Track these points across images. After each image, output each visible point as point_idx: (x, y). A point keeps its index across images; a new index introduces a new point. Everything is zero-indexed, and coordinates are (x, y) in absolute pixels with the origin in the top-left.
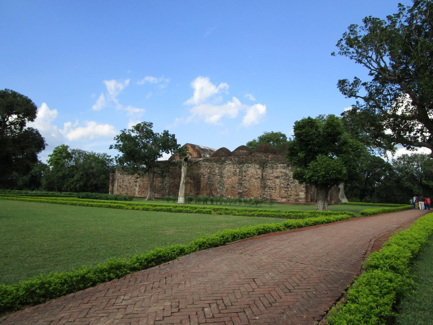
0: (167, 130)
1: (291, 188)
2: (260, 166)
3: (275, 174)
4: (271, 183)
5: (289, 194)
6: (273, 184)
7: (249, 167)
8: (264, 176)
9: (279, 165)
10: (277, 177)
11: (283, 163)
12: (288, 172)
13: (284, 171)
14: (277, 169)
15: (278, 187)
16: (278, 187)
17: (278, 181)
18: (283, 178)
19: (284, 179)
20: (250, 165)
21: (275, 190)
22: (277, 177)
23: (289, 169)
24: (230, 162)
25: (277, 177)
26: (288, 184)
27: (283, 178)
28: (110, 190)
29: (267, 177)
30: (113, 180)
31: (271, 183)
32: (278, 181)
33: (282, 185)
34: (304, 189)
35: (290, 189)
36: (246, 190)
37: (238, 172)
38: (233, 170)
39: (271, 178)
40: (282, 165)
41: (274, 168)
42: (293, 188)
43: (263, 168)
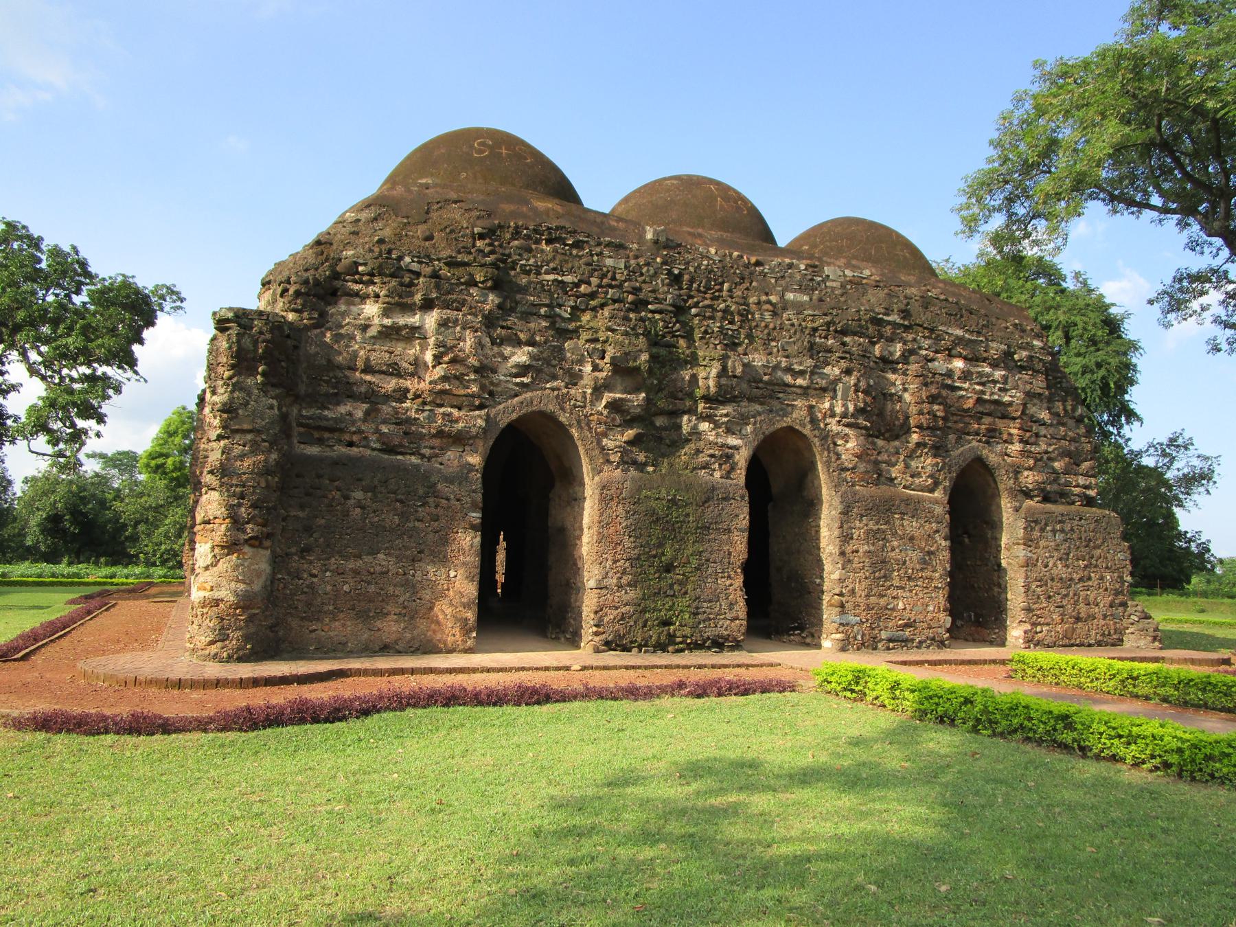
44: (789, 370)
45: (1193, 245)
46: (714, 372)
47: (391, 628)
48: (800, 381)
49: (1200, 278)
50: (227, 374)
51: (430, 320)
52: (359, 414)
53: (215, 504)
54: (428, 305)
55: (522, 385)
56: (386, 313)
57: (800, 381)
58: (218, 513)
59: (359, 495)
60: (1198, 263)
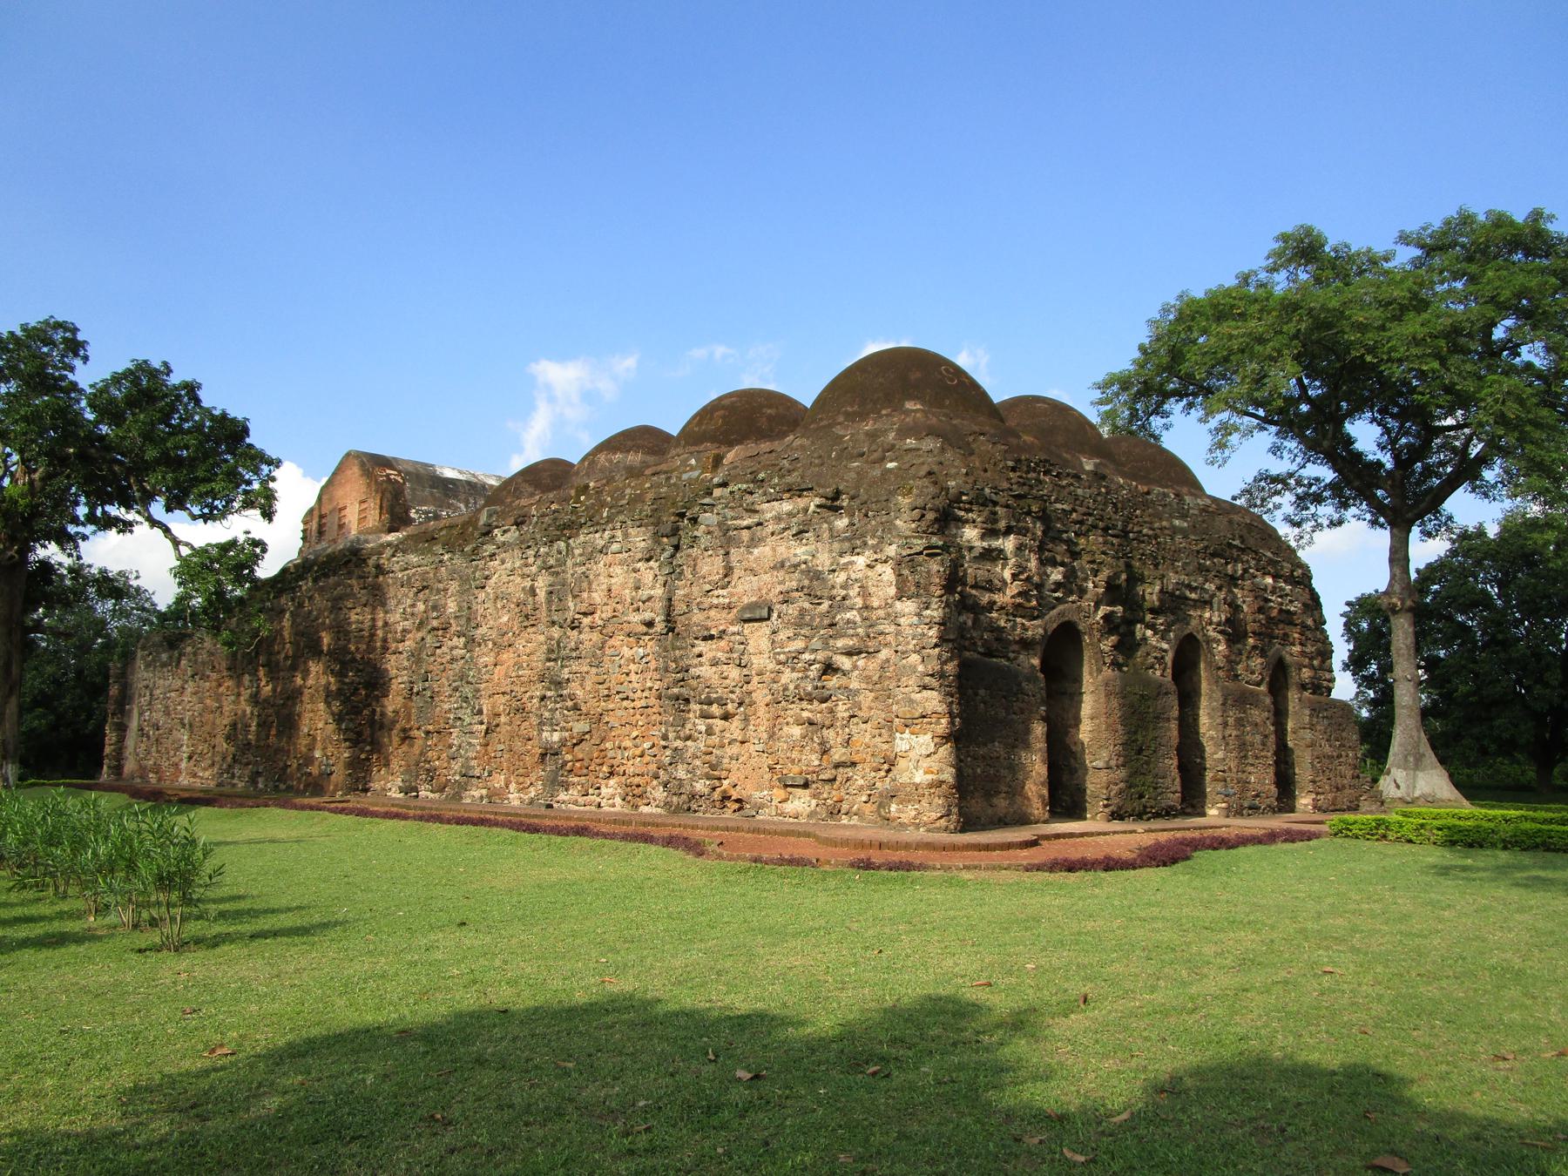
0: (141, 358)
1: (851, 694)
2: (657, 536)
3: (745, 589)
4: (715, 663)
5: (838, 754)
6: (734, 673)
7: (591, 555)
8: (680, 607)
9: (770, 510)
10: (752, 607)
11: (797, 491)
12: (823, 561)
13: (800, 551)
14: (754, 542)
15: (761, 696)
16: (761, 696)
17: (758, 637)
18: (792, 610)
19: (800, 622)
20: (599, 540)
21: (746, 719)
22: (757, 614)
23: (834, 535)
24: (513, 535)
25: (757, 614)
26: (829, 669)
27: (792, 610)
28: (107, 750)
29: (697, 617)
30: (125, 699)
31: (715, 663)
32: (765, 644)
33: (788, 677)
34: (933, 701)
35: (842, 711)
36: (580, 727)
37: (542, 595)
38: (517, 586)
39: (719, 620)
40: (786, 506)
41: (737, 543)
42: (866, 698)
43: (677, 548)
44: (1189, 587)
45: (1275, 450)
46: (1157, 588)
47: (1001, 803)
48: (1193, 596)
49: (1275, 479)
50: (939, 593)
51: (1009, 544)
52: (970, 623)
53: (935, 702)
54: (1008, 531)
55: (1057, 599)
56: (983, 537)
57: (1193, 596)
58: (940, 710)
59: (982, 692)
60: (1279, 467)
